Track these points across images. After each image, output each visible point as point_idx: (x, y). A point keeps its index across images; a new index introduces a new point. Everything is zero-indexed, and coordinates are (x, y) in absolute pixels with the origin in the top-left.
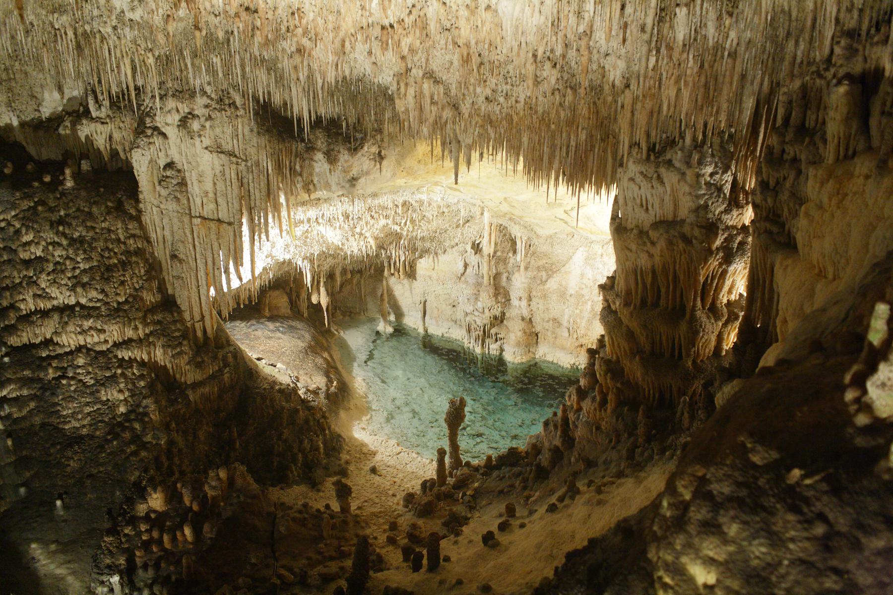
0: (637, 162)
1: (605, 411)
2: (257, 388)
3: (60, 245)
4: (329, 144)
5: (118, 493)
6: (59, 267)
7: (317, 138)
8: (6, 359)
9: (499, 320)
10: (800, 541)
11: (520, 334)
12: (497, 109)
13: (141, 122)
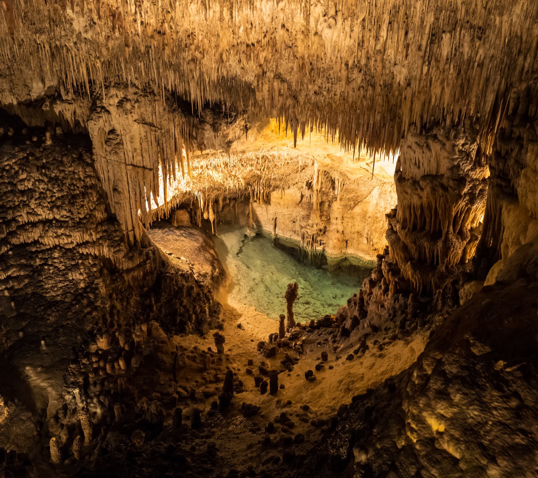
0: (414, 135)
1: (387, 295)
2: (167, 273)
3: (43, 181)
4: (214, 119)
5: (79, 337)
6: (42, 196)
7: (207, 115)
8: (10, 253)
9: (324, 231)
10: (500, 410)
11: (335, 241)
12: (322, 99)
13: (94, 104)
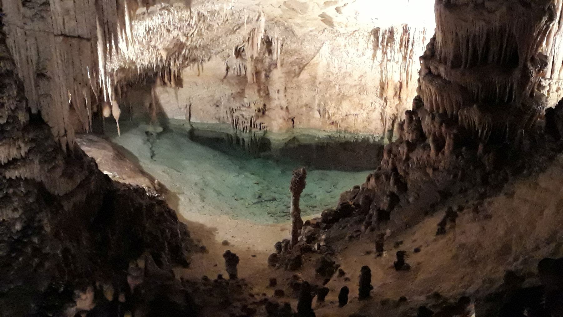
9: (262, 111)
11: (281, 121)
